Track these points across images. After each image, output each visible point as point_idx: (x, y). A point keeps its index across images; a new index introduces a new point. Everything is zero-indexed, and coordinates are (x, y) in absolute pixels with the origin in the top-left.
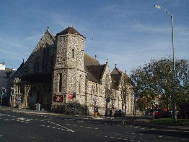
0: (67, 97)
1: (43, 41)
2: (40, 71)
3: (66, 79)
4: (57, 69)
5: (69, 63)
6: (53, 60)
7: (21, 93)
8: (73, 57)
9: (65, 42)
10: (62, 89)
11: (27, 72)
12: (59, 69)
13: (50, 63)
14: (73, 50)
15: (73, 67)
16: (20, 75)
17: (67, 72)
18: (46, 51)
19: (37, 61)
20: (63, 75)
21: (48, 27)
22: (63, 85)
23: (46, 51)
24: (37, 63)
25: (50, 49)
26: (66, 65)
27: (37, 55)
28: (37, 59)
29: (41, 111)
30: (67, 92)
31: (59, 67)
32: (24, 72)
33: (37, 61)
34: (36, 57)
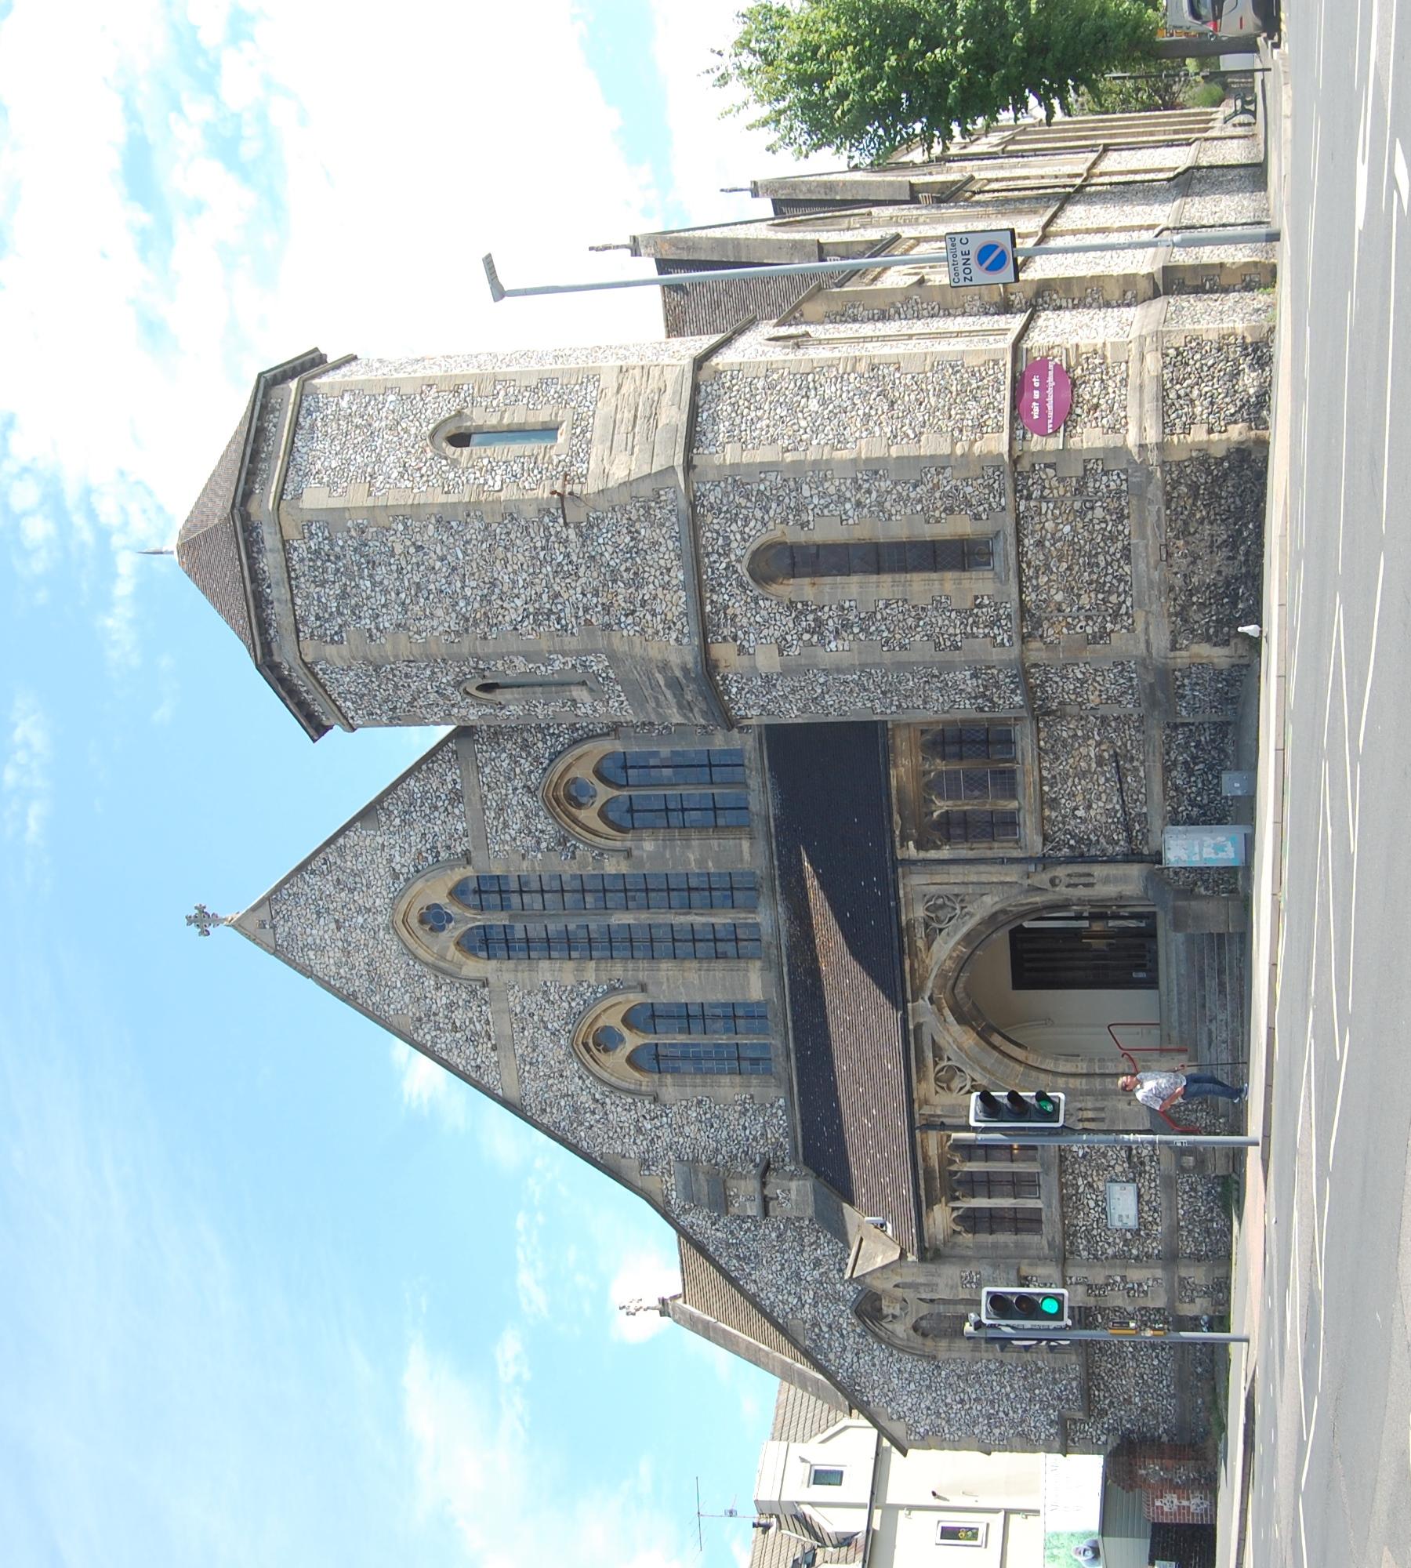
0: (1055, 443)
1: (374, 977)
2: (754, 984)
3: (821, 469)
4: (705, 629)
5: (613, 465)
6: (603, 814)
7: (1019, 1185)
8: (548, 431)
9: (354, 545)
10: (958, 526)
11: (766, 1169)
12: (698, 587)
13: (649, 846)
14: (460, 440)
15: (673, 415)
16: (810, 1275)
17: (738, 479)
18: (499, 919)
19: (633, 1040)
20: (777, 532)
21: (202, 920)
22: (900, 526)
23: (499, 919)
24: (650, 1039)
25: (467, 857)
26: (643, 496)
27: (544, 1042)
28: (605, 1040)
29: (1243, 812)
30: (998, 443)
31: (676, 602)
32: (765, 1201)
33: (633, 1040)
34: (572, 1053)
